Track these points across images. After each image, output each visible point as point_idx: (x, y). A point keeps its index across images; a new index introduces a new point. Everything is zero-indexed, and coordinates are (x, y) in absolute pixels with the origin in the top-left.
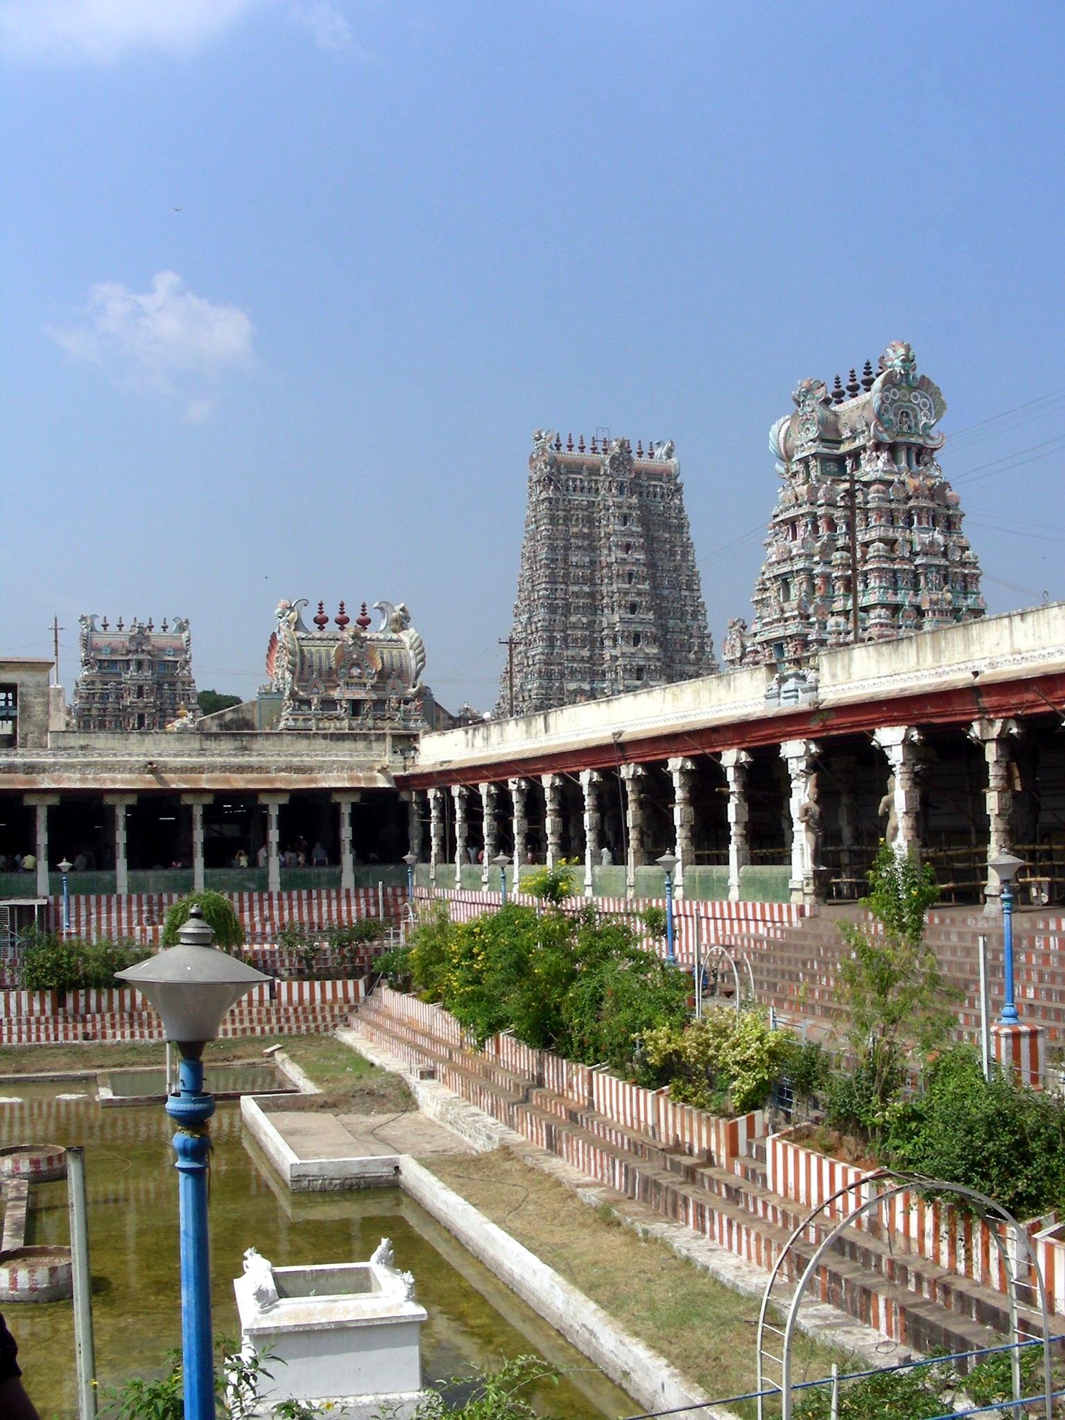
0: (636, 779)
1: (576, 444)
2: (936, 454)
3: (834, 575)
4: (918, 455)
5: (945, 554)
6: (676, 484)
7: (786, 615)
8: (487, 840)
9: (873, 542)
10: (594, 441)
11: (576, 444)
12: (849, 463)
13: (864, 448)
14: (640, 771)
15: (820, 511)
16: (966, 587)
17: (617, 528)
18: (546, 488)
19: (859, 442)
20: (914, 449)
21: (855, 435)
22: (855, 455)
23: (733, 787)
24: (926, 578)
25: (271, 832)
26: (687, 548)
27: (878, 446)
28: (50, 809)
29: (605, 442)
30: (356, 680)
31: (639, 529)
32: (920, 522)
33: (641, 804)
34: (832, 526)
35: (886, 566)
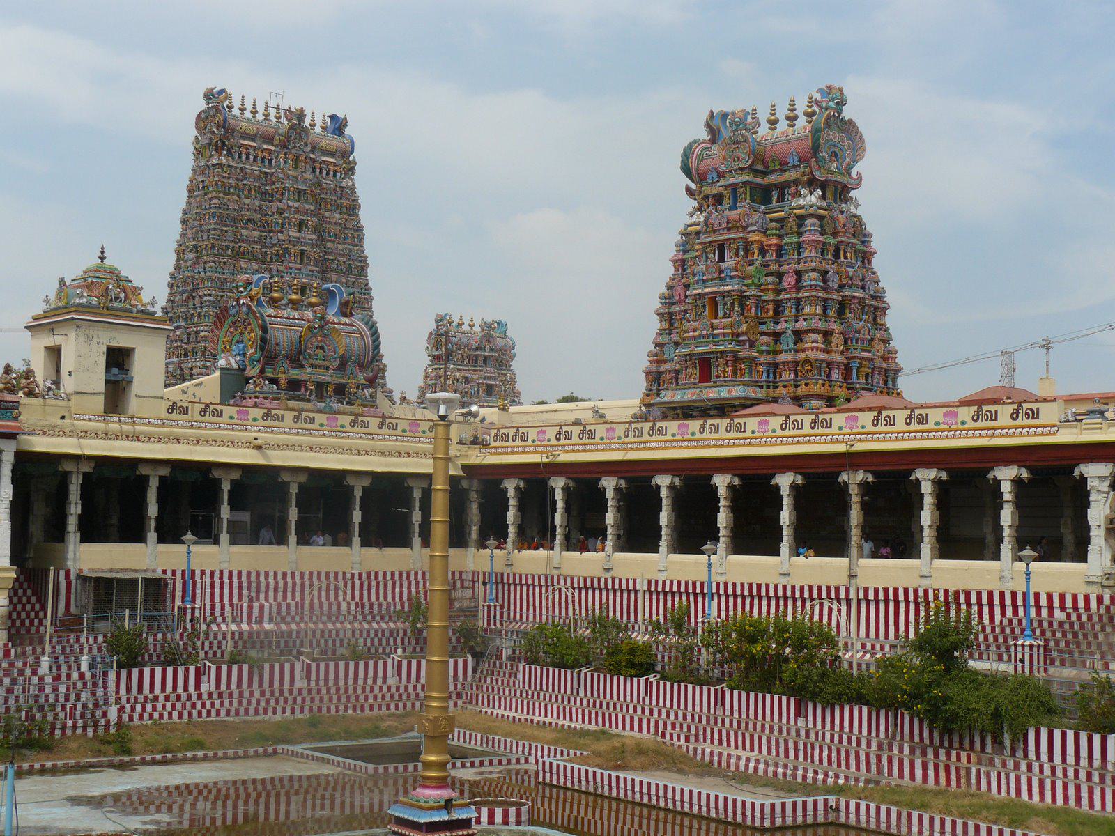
0: (864, 485)
1: (249, 107)
2: (853, 194)
3: (766, 298)
4: (841, 192)
5: (863, 288)
6: (350, 163)
7: (716, 332)
8: (610, 531)
9: (807, 271)
10: (267, 107)
11: (249, 107)
12: (775, 194)
13: (796, 182)
14: (870, 478)
15: (754, 237)
16: (875, 319)
17: (290, 203)
18: (219, 150)
19: (786, 176)
20: (840, 188)
21: (784, 166)
22: (783, 187)
23: (1007, 497)
24: (850, 308)
25: (355, 512)
26: (357, 234)
27: (812, 183)
28: (162, 480)
29: (278, 108)
30: (320, 362)
31: (312, 208)
32: (845, 257)
33: (865, 507)
34: (763, 252)
35: (820, 295)
